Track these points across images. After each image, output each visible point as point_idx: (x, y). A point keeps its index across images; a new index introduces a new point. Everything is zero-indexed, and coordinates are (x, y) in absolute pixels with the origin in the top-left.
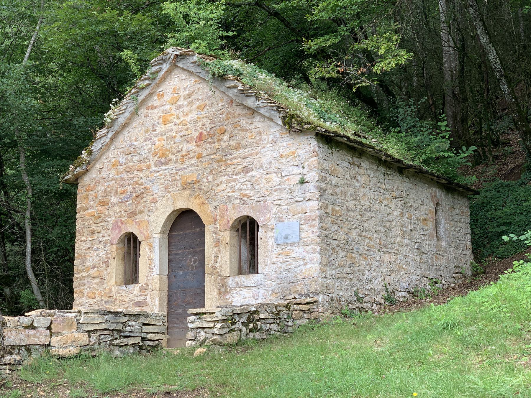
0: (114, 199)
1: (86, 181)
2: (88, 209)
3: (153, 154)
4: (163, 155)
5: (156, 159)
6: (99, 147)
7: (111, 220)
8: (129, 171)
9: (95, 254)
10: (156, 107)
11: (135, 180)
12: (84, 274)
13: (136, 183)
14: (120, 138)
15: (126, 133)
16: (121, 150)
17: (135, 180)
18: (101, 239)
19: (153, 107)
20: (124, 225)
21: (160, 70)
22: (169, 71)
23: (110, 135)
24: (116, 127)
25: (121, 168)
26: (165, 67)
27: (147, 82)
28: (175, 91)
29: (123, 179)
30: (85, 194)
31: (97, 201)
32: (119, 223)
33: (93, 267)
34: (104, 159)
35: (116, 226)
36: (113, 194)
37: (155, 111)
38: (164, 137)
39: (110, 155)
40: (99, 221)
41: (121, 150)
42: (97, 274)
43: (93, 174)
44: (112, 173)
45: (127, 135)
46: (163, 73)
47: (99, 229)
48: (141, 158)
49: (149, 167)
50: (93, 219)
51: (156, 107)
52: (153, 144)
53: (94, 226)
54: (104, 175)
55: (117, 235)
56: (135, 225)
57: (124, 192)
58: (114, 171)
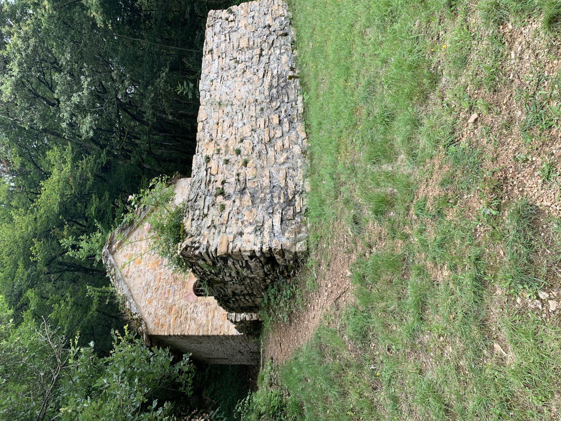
0: (170, 301)
1: (151, 326)
2: (170, 324)
3: (154, 271)
4: (157, 263)
5: (157, 268)
6: (135, 309)
7: (183, 302)
8: (157, 289)
9: (200, 315)
10: (129, 270)
11: (164, 284)
12: (210, 324)
13: (166, 282)
14: (135, 297)
15: (134, 292)
16: (143, 296)
17: (164, 284)
18: (192, 310)
19: (128, 272)
20: (188, 291)
21: (110, 261)
22: (113, 258)
23: (131, 300)
24: (128, 295)
25: (154, 295)
26: (110, 258)
27: (113, 269)
28: (125, 256)
29: (161, 293)
30: (160, 327)
31: (168, 316)
32: (186, 295)
33: (208, 316)
34: (143, 310)
35: (187, 298)
36: (167, 301)
37: (130, 270)
38: (148, 262)
39: (143, 305)
40: (180, 313)
41: (143, 296)
42: (212, 312)
43: (149, 319)
44: (154, 303)
45: (136, 292)
46: (112, 260)
47: (185, 312)
48: (153, 280)
49: (160, 273)
50: (178, 318)
51: (129, 270)
52: (148, 271)
53: (182, 318)
54: (153, 310)
55: (193, 296)
56: (190, 282)
57: (169, 292)
58: (154, 302)
